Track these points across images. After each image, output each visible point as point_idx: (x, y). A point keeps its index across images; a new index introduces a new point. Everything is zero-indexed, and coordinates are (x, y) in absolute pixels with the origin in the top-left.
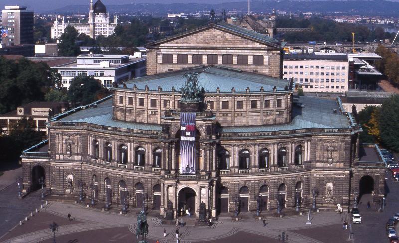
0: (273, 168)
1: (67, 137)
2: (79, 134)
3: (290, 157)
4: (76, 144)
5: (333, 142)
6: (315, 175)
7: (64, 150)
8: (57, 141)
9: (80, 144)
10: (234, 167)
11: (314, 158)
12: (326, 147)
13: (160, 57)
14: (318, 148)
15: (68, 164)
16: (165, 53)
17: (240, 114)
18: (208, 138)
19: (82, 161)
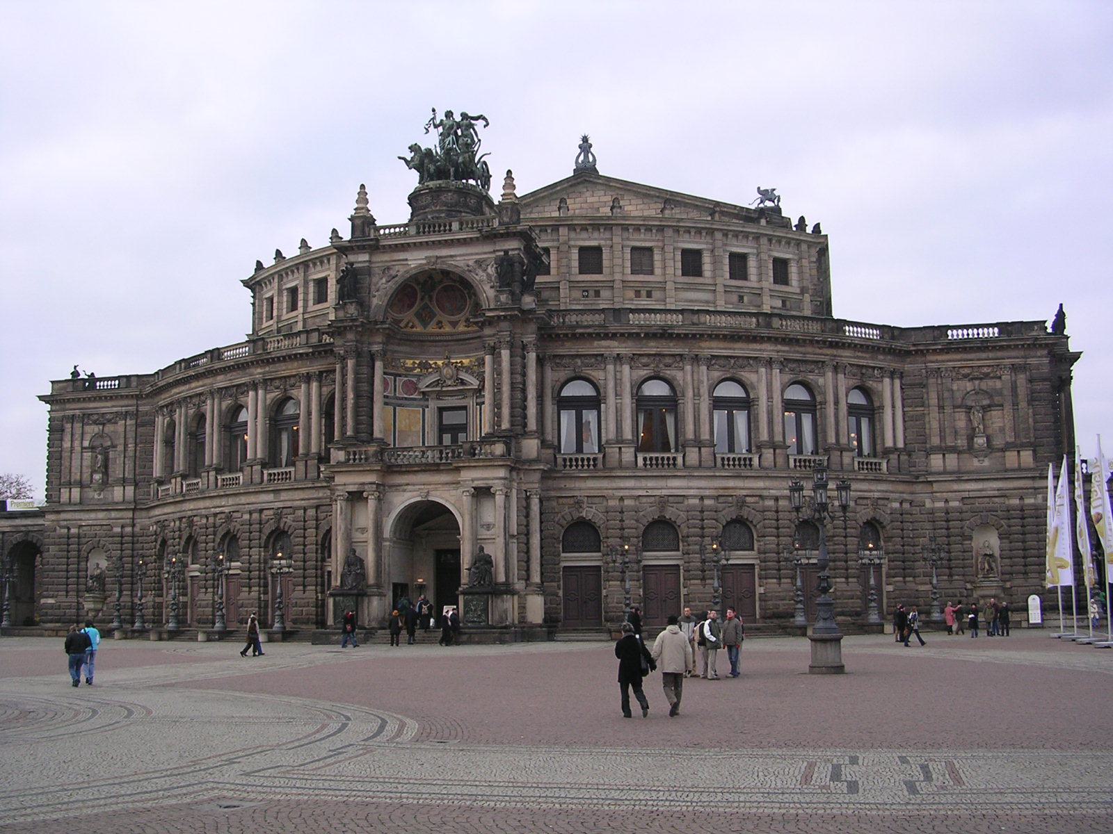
0: (768, 454)
1: (96, 429)
3: (831, 420)
4: (120, 448)
5: (987, 376)
6: (928, 504)
7: (85, 470)
8: (67, 444)
9: (131, 446)
10: (620, 441)
11: (918, 444)
12: (958, 395)
14: (934, 401)
15: (93, 515)
17: (644, 293)
18: (503, 298)
19: (137, 507)
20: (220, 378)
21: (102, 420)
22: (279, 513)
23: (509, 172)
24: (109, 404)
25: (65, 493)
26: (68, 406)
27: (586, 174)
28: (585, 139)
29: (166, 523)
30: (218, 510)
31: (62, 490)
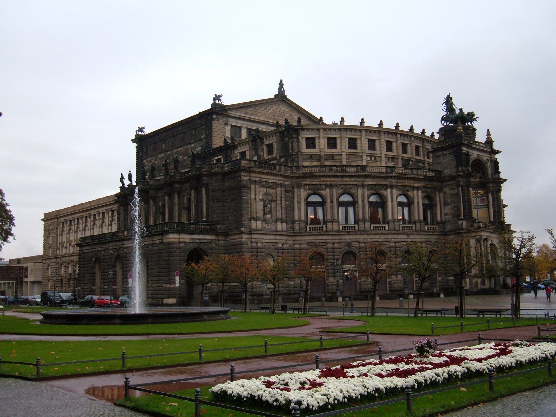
1: (265, 190)
2: (281, 185)
4: (278, 202)
8: (253, 196)
13: (228, 128)
15: (268, 237)
16: (233, 124)
20: (367, 179)
21: (268, 186)
22: (408, 244)
23: (488, 130)
24: (272, 177)
25: (253, 224)
26: (252, 175)
27: (280, 97)
28: (281, 81)
29: (321, 244)
30: (373, 240)
31: (252, 222)
